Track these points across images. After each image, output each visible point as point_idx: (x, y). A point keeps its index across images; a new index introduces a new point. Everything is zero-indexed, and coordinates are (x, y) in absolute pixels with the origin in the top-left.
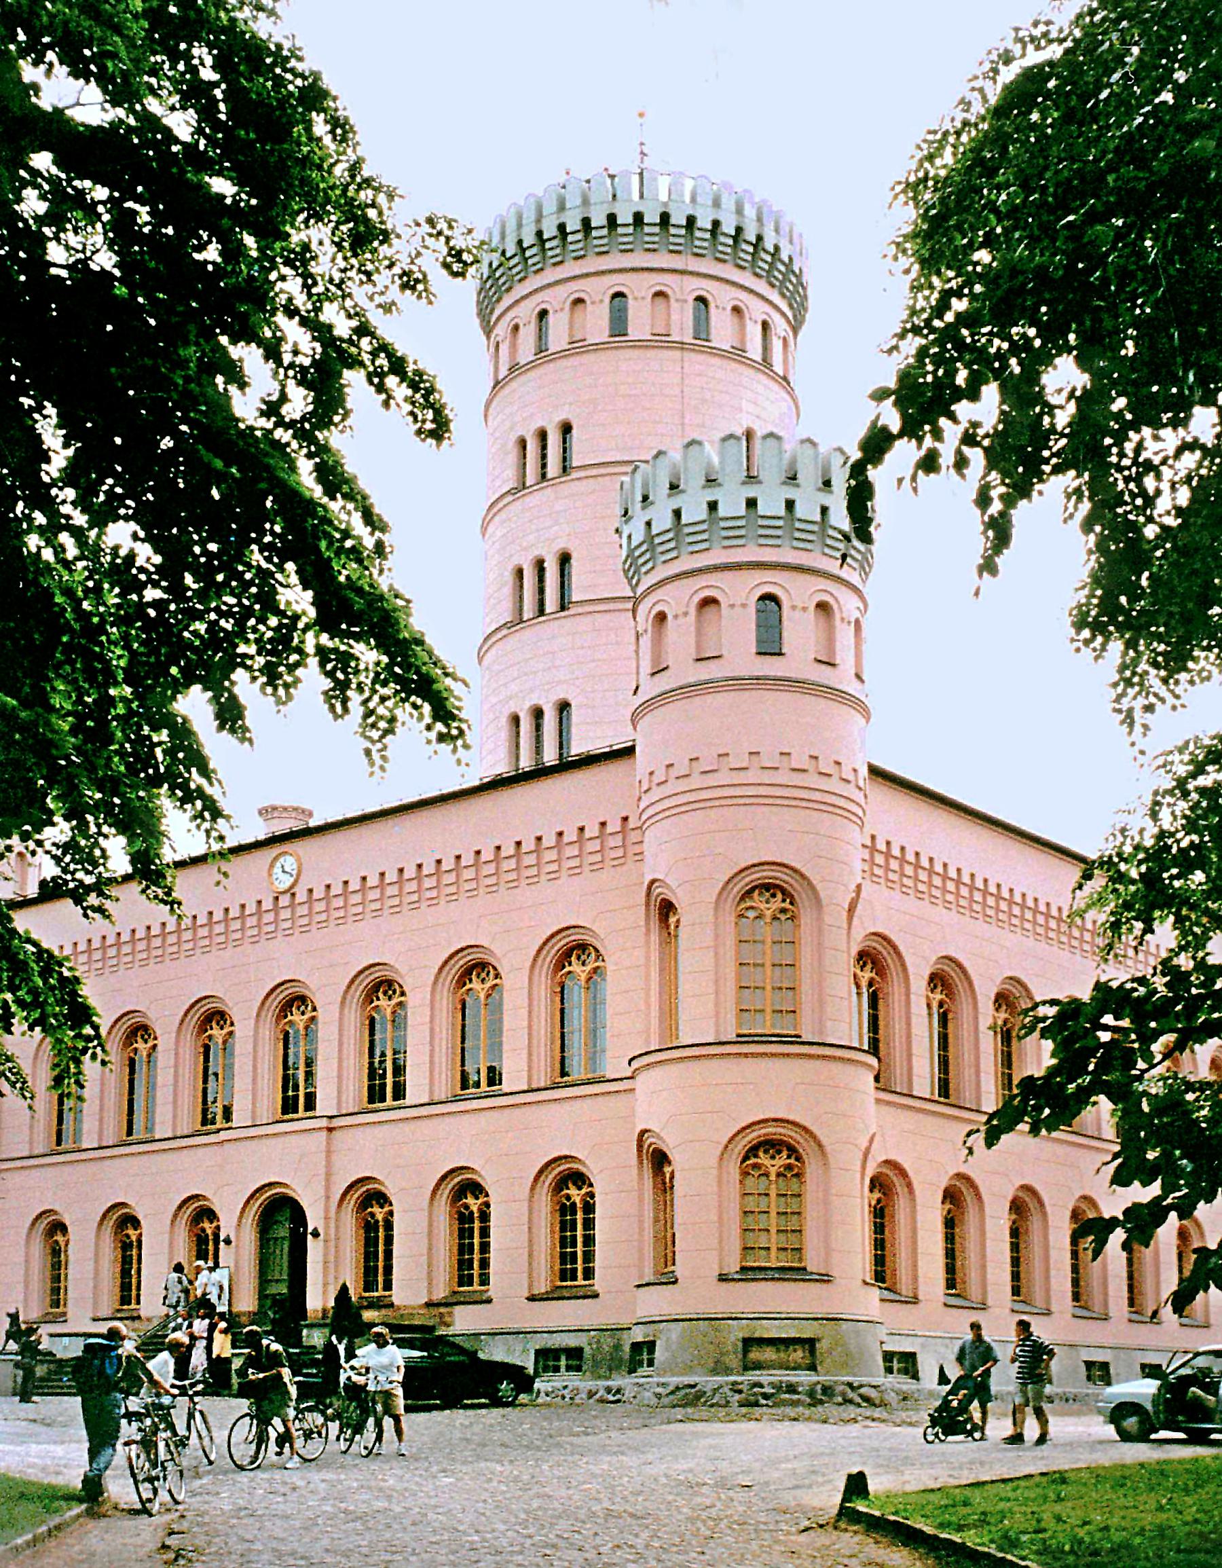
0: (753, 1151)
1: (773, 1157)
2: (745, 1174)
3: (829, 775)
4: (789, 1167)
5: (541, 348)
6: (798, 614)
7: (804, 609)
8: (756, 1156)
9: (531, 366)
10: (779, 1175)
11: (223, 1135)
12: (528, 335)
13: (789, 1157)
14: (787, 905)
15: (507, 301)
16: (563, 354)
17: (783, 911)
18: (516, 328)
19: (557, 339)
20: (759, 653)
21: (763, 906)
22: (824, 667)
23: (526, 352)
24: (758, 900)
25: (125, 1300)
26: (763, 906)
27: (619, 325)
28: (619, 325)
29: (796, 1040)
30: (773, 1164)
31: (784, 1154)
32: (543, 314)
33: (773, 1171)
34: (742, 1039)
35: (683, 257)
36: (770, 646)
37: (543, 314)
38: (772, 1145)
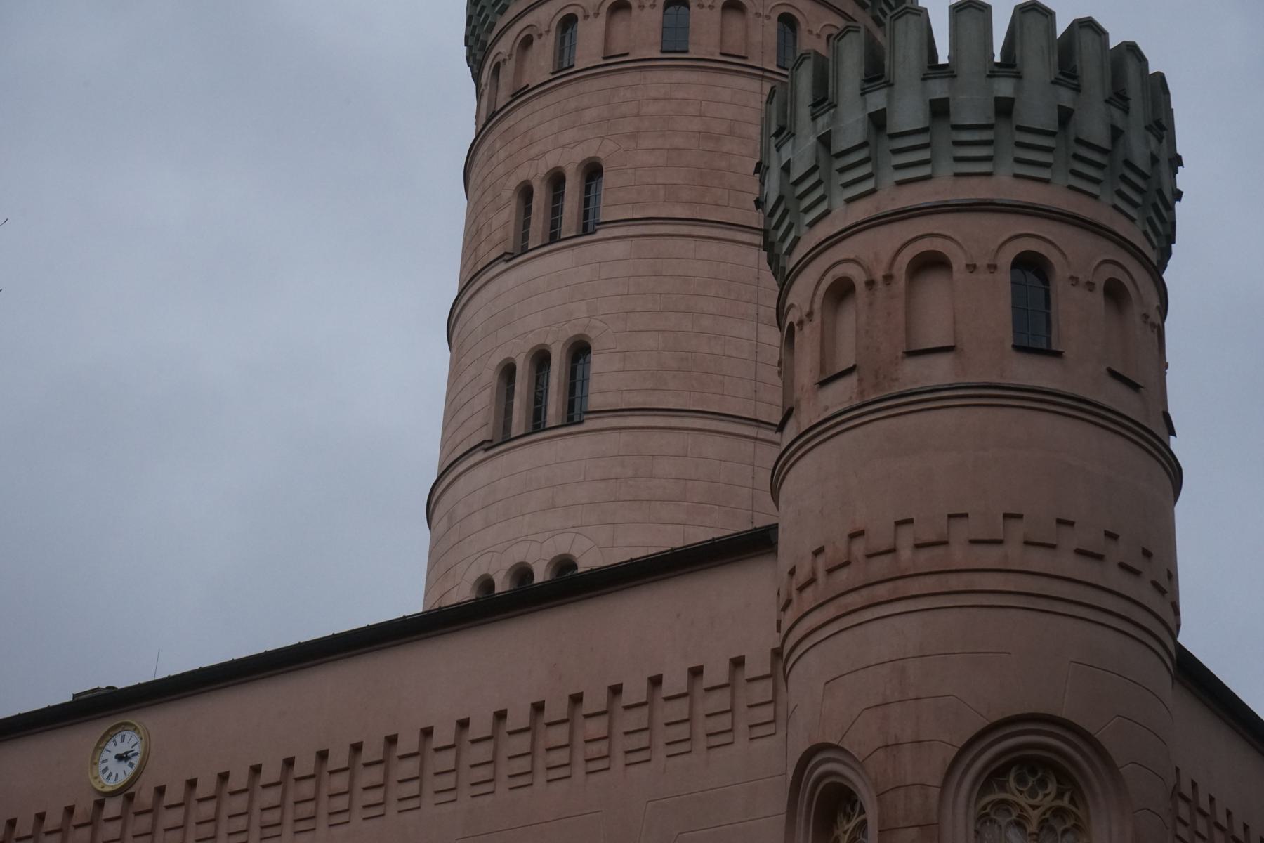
3: (1135, 572)
5: (563, 68)
7: (1090, 286)
9: (543, 88)
14: (1065, 802)
16: (593, 72)
17: (1059, 812)
18: (527, 42)
20: (1018, 348)
21: (1023, 800)
23: (541, 61)
24: (1013, 792)
26: (1023, 800)
32: (568, 22)
37: (568, 22)
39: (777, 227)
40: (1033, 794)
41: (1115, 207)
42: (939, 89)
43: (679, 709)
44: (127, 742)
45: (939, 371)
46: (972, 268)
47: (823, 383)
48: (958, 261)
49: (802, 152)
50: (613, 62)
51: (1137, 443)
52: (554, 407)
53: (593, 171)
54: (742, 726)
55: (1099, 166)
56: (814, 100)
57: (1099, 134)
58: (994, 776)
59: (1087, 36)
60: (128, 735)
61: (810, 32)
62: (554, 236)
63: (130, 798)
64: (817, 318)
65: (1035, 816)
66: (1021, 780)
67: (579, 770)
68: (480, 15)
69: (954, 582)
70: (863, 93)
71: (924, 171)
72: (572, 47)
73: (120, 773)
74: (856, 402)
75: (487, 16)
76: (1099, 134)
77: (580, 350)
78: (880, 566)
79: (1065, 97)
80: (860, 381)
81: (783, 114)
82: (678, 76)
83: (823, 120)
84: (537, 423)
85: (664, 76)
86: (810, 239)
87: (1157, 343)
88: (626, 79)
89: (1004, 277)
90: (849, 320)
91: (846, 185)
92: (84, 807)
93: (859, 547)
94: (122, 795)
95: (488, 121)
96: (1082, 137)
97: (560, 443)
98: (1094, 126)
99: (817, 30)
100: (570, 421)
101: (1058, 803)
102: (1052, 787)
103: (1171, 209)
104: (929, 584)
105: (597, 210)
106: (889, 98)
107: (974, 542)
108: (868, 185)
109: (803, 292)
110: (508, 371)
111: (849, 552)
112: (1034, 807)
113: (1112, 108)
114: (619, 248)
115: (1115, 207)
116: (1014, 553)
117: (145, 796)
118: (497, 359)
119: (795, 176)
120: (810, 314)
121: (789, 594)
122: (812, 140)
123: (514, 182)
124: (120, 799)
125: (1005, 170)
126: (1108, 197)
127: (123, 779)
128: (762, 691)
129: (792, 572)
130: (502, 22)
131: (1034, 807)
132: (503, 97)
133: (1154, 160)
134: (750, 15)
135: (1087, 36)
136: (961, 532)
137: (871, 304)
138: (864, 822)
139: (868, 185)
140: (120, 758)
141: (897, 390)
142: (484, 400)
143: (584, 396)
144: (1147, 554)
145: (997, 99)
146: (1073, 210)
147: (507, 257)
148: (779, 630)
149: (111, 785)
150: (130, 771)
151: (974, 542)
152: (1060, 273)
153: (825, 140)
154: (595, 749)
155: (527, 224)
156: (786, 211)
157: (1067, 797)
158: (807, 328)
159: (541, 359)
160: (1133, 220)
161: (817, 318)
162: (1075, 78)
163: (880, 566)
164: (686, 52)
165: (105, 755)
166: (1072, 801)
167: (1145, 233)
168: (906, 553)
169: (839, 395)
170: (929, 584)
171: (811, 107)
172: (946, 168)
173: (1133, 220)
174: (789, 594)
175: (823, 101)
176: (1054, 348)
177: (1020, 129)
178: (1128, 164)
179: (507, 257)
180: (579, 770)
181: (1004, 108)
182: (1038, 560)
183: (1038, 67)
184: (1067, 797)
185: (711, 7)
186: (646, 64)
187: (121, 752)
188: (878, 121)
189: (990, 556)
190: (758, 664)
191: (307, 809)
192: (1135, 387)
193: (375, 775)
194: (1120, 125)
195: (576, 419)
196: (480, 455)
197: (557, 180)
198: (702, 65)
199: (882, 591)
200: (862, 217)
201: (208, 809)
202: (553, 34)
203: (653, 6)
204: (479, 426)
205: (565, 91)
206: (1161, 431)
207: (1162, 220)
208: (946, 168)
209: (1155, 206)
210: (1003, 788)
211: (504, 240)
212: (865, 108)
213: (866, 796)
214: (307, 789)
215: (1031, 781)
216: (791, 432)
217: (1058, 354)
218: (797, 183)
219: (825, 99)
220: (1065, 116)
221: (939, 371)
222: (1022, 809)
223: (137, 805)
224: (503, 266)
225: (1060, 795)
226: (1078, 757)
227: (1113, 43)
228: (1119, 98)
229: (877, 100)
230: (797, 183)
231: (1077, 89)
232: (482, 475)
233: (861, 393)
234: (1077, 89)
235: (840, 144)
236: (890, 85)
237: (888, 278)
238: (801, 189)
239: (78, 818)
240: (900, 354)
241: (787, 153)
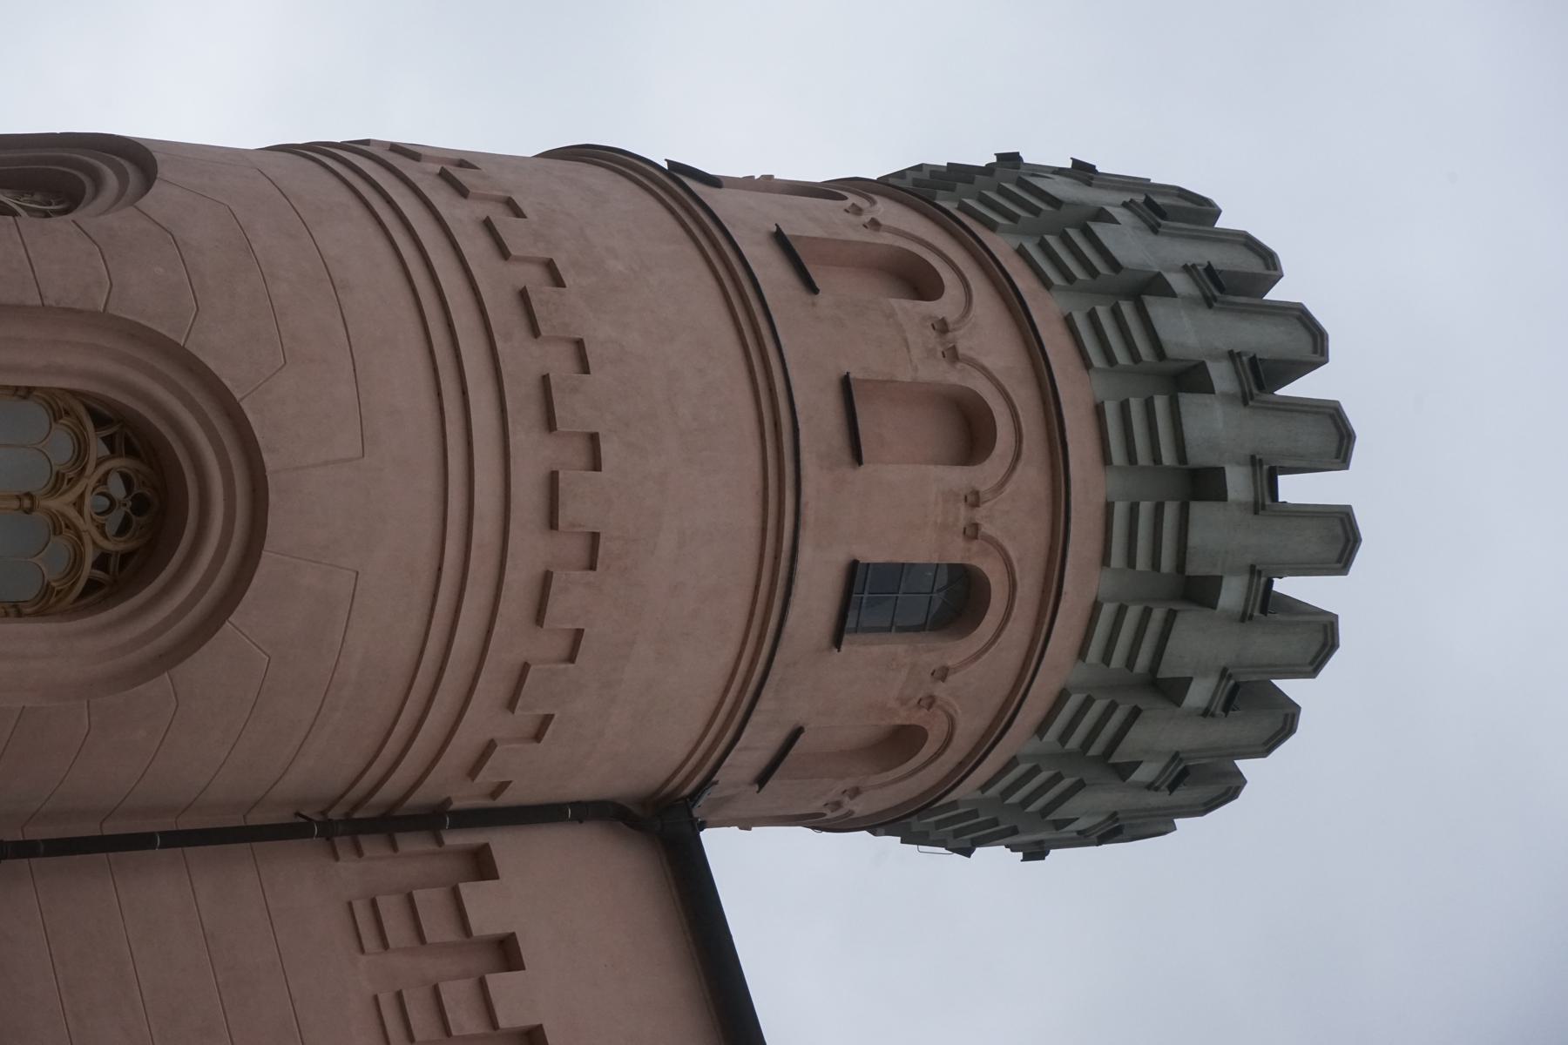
42: (1238, 483)
56: (1221, 272)
70: (1233, 356)
87: (781, 813)
91: (1092, 317)
119: (1099, 229)
126: (1034, 745)
153: (1156, 285)
162: (1227, 707)
171: (1206, 264)
219: (1221, 289)
229: (1221, 375)
235: (1158, 309)
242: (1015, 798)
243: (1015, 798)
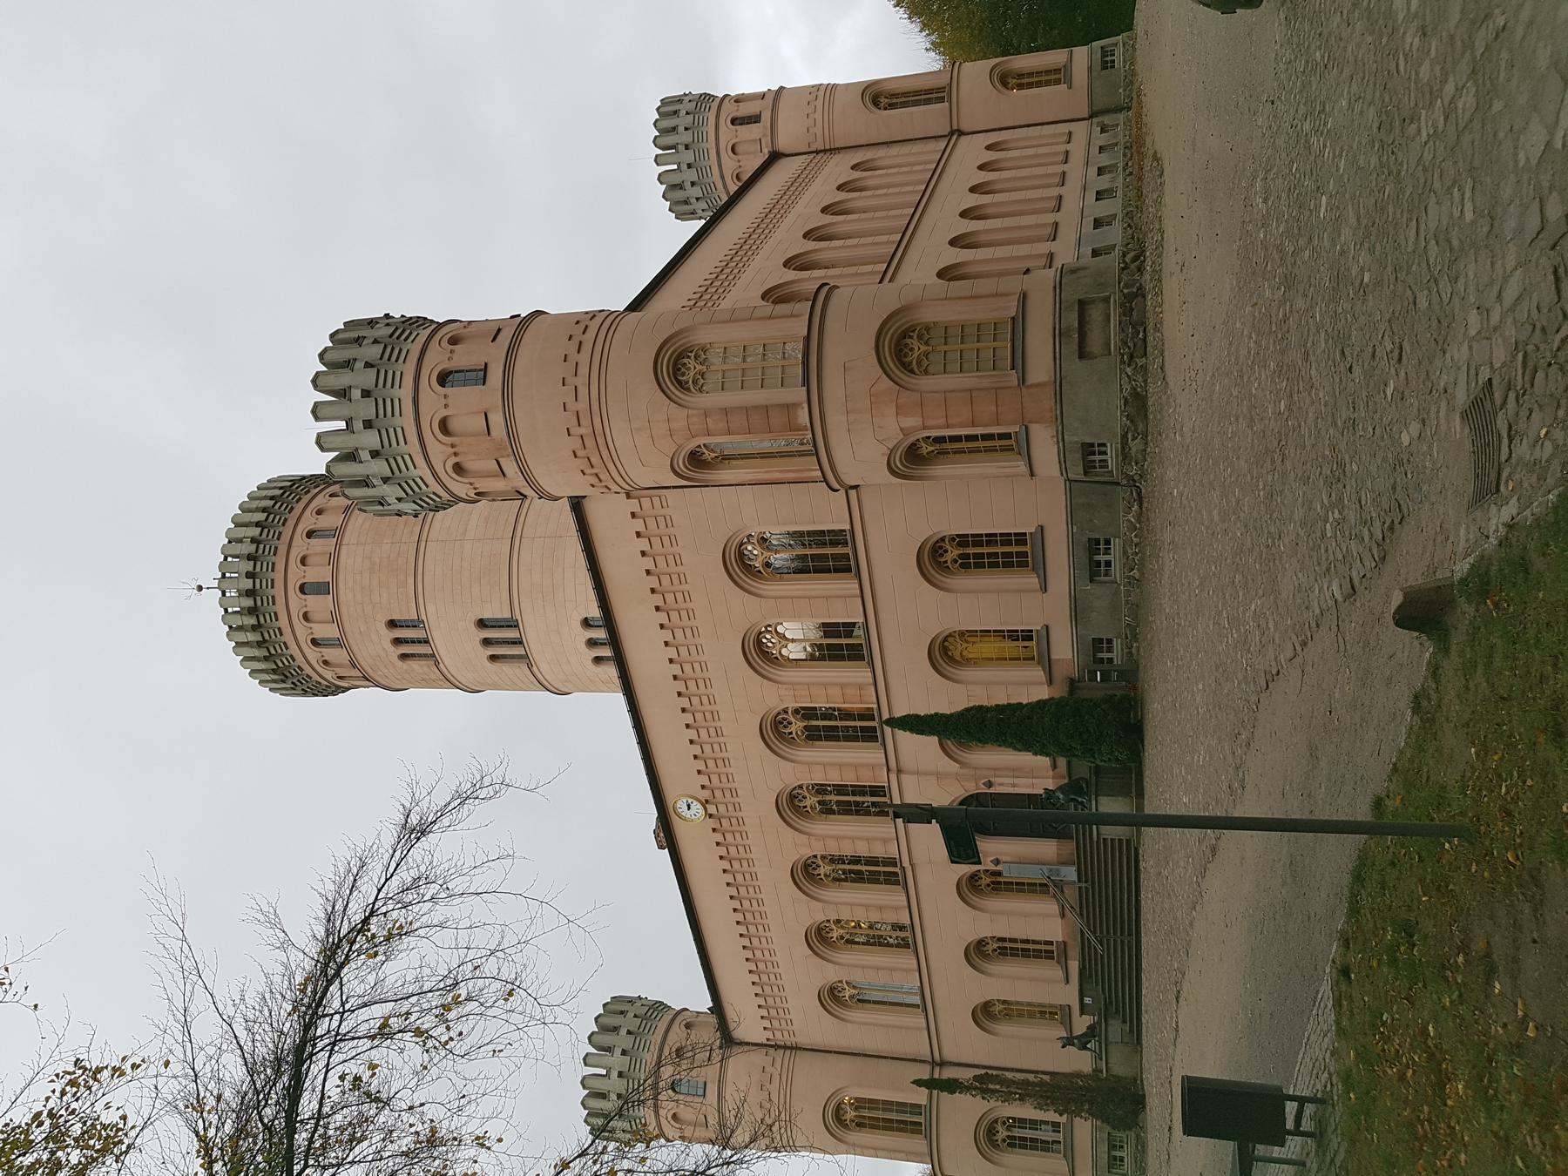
0: (907, 367)
1: (912, 350)
2: (926, 372)
3: (587, 326)
4: (920, 337)
5: (338, 643)
6: (455, 357)
8: (911, 363)
10: (927, 344)
11: (906, 863)
12: (331, 654)
13: (911, 337)
14: (692, 355)
15: (308, 670)
16: (341, 626)
18: (326, 662)
19: (330, 631)
21: (692, 374)
22: (499, 337)
24: (689, 377)
25: (1049, 955)
27: (322, 588)
28: (322, 588)
29: (808, 339)
30: (917, 347)
31: (908, 341)
32: (315, 642)
33: (923, 348)
34: (806, 382)
35: (280, 547)
36: (481, 375)
37: (315, 642)
38: (900, 352)
39: (428, 504)
40: (689, 369)
41: (412, 342)
42: (358, 425)
43: (656, 542)
44: (682, 806)
45: (497, 419)
46: (446, 406)
47: (504, 475)
48: (444, 413)
49: (391, 492)
50: (336, 618)
51: (525, 330)
52: (511, 634)
53: (392, 624)
54: (663, 512)
55: (393, 349)
57: (378, 349)
58: (682, 386)
59: (327, 357)
60: (679, 806)
61: (315, 523)
62: (427, 642)
63: (707, 801)
64: (472, 480)
65: (699, 367)
66: (683, 375)
67: (685, 587)
68: (312, 689)
69: (595, 407)
71: (399, 431)
72: (328, 639)
73: (697, 807)
74: (513, 458)
75: (313, 685)
76: (378, 349)
77: (482, 624)
78: (589, 442)
79: (359, 365)
80: (503, 457)
81: (370, 503)
82: (341, 585)
83: (375, 482)
84: (518, 642)
85: (341, 592)
86: (434, 486)
88: (344, 610)
89: (448, 390)
90: (471, 464)
92: (713, 823)
93: (580, 453)
94: (707, 805)
95: (370, 681)
96: (379, 357)
97: (527, 629)
98: (373, 352)
99: (314, 520)
100: (517, 626)
101: (692, 357)
102: (686, 360)
103: (411, 318)
104: (597, 421)
105: (412, 620)
106: (363, 449)
107: (576, 400)
108: (407, 458)
109: (461, 488)
110: (493, 658)
111: (584, 457)
112: (695, 368)
113: (364, 343)
114: (430, 608)
115: (412, 342)
116: (581, 381)
117: (706, 794)
118: (488, 664)
119: (404, 495)
120: (471, 484)
121: (603, 487)
122: (385, 486)
123: (399, 663)
124: (707, 805)
125: (396, 392)
126: (408, 345)
127: (699, 806)
128: (646, 502)
129: (593, 486)
130: (316, 677)
131: (695, 368)
132: (355, 673)
133: (388, 325)
134: (308, 552)
135: (327, 357)
136: (572, 405)
137: (466, 453)
138: (704, 445)
139: (407, 458)
140: (689, 809)
141: (506, 438)
142: (505, 669)
143: (505, 620)
144: (578, 322)
145: (362, 397)
146: (415, 360)
147: (437, 664)
148: (619, 493)
149: (702, 812)
150: (695, 803)
151: (576, 400)
152: (446, 365)
153: (385, 480)
154: (676, 580)
155: (420, 655)
156: (420, 499)
157: (690, 354)
158: (477, 485)
159: (487, 642)
160: (418, 334)
161: (472, 480)
163: (589, 442)
164: (329, 583)
165: (688, 816)
166: (691, 352)
167: (424, 329)
168: (583, 431)
169: (510, 466)
170: (597, 421)
172: (397, 421)
173: (418, 334)
174: (603, 487)
175: (365, 483)
176: (483, 367)
177: (376, 386)
178: (391, 336)
179: (437, 664)
180: (685, 587)
181: (366, 394)
182: (583, 370)
183: (343, 379)
184: (690, 354)
185: (305, 572)
186: (336, 602)
187: (687, 808)
188: (375, 454)
189: (583, 391)
190: (634, 505)
191: (708, 716)
192: (499, 330)
193: (692, 684)
194: (372, 340)
195: (516, 624)
196: (535, 669)
197: (398, 642)
198: (335, 573)
199: (601, 441)
200: (422, 458)
201: (711, 763)
202: (320, 650)
203: (305, 600)
204: (520, 670)
205: (351, 640)
206: (519, 320)
207: (417, 321)
208: (397, 421)
209: (410, 324)
210: (687, 382)
211: (428, 666)
212: (369, 461)
213: (692, 445)
214: (699, 716)
215: (683, 370)
216: (528, 491)
217: (486, 364)
218: (407, 494)
220: (368, 365)
221: (497, 419)
222: (696, 373)
223: (710, 798)
224: (441, 665)
225: (689, 357)
226: (672, 349)
227: (331, 345)
228: (358, 341)
229: (365, 455)
230: (407, 494)
231: (355, 360)
232: (544, 667)
233: (508, 456)
234: (355, 360)
236: (357, 449)
237: (453, 446)
238: (410, 492)
239: (717, 826)
240: (489, 438)
241: (392, 500)
242: (408, 332)
243: (408, 332)
